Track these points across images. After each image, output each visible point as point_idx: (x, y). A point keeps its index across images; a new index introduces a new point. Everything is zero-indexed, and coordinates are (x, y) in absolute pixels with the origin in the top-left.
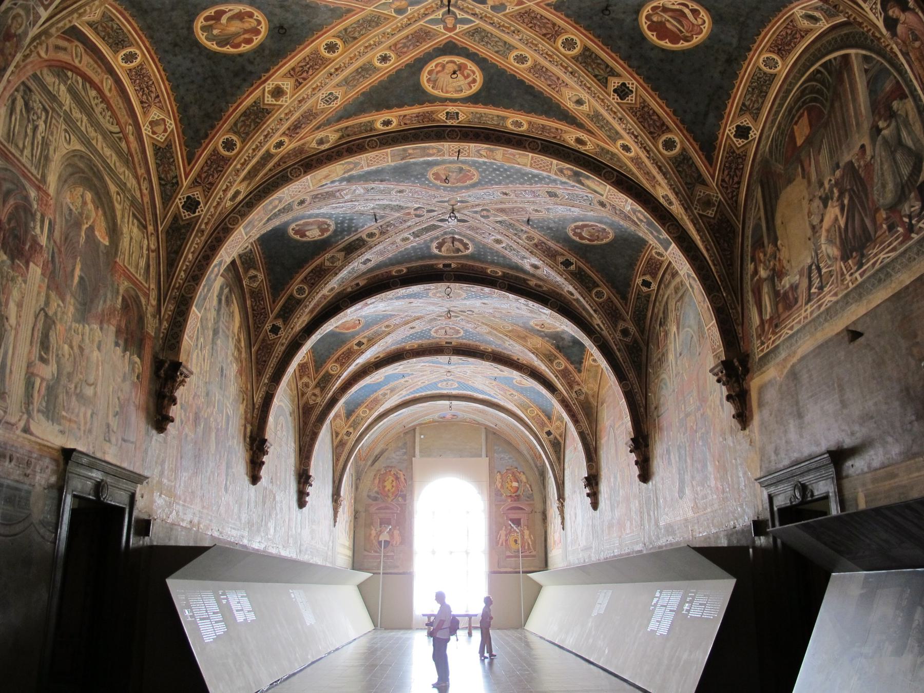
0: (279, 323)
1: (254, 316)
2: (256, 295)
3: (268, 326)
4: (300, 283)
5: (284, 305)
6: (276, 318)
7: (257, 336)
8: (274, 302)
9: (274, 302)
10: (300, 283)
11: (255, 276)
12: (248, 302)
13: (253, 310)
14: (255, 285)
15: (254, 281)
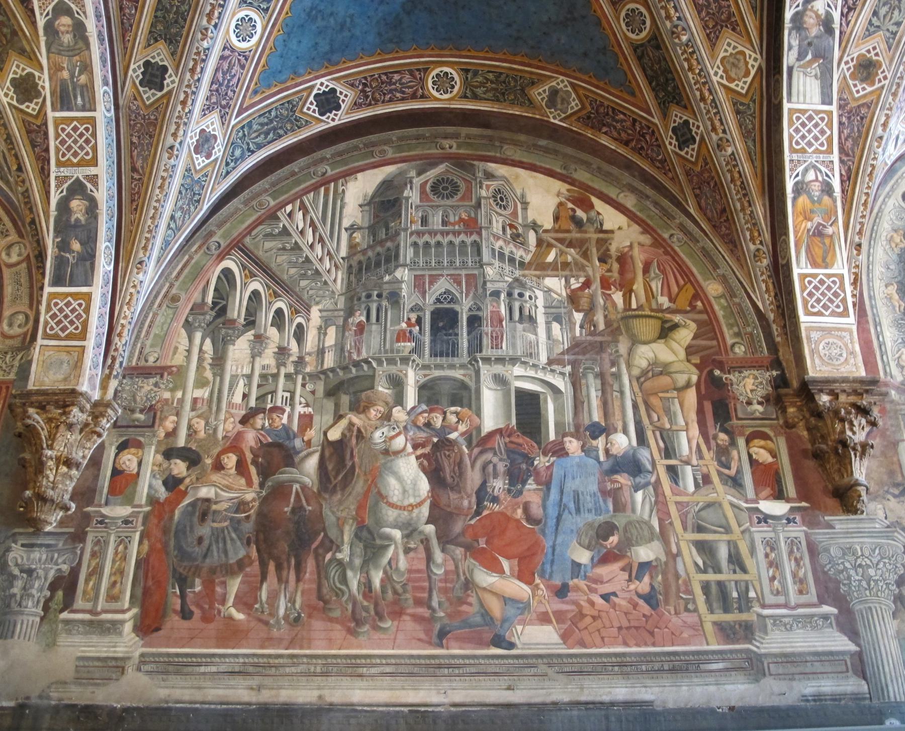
0: (678, 116)
1: (638, 151)
2: (597, 116)
3: (670, 144)
4: (617, 12)
5: (650, 80)
6: (665, 115)
7: (674, 179)
8: (633, 94)
9: (633, 94)
10: (617, 12)
11: (554, 93)
12: (605, 141)
13: (626, 143)
14: (574, 104)
15: (566, 101)
